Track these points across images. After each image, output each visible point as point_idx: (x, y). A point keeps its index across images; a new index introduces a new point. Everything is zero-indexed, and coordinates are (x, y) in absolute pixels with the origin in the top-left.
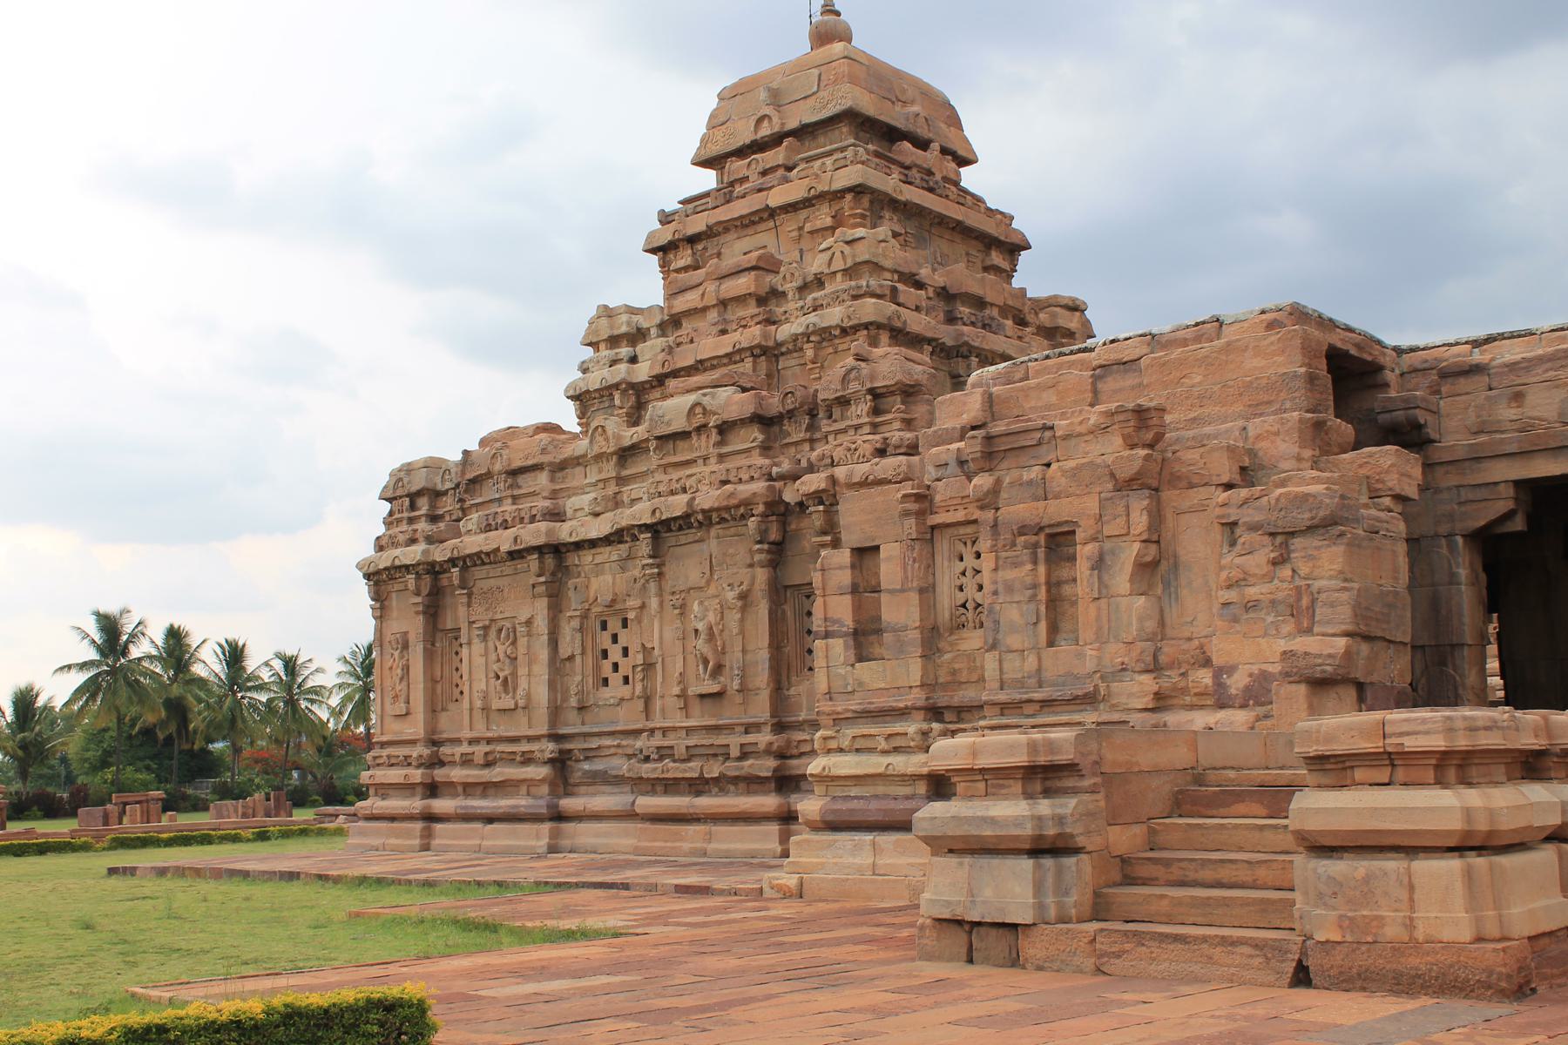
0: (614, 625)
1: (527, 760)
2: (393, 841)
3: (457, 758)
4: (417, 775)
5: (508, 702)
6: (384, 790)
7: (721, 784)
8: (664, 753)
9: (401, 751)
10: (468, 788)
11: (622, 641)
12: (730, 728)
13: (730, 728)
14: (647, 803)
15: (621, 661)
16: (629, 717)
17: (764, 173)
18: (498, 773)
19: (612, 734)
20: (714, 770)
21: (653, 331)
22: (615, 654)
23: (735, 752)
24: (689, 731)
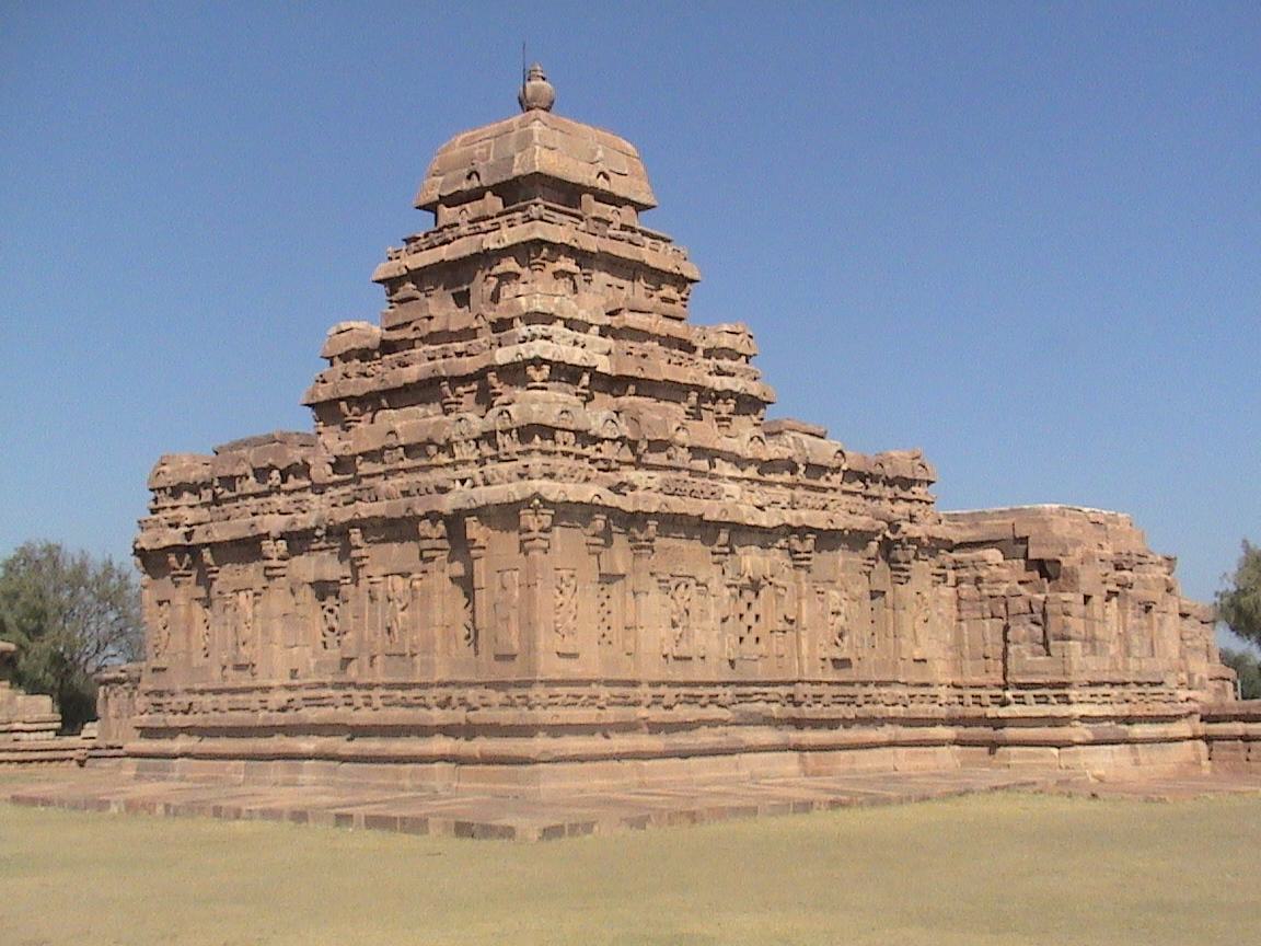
0: (749, 595)
1: (713, 699)
2: (598, 782)
3: (649, 700)
4: (612, 714)
5: (683, 650)
6: (556, 730)
7: (847, 723)
8: (818, 698)
9: (584, 691)
10: (655, 728)
11: (757, 607)
12: (852, 684)
13: (852, 684)
14: (810, 736)
15: (754, 625)
16: (761, 672)
17: (624, 228)
18: (684, 713)
19: (755, 684)
20: (852, 712)
21: (596, 329)
22: (749, 619)
23: (860, 700)
24: (829, 683)
